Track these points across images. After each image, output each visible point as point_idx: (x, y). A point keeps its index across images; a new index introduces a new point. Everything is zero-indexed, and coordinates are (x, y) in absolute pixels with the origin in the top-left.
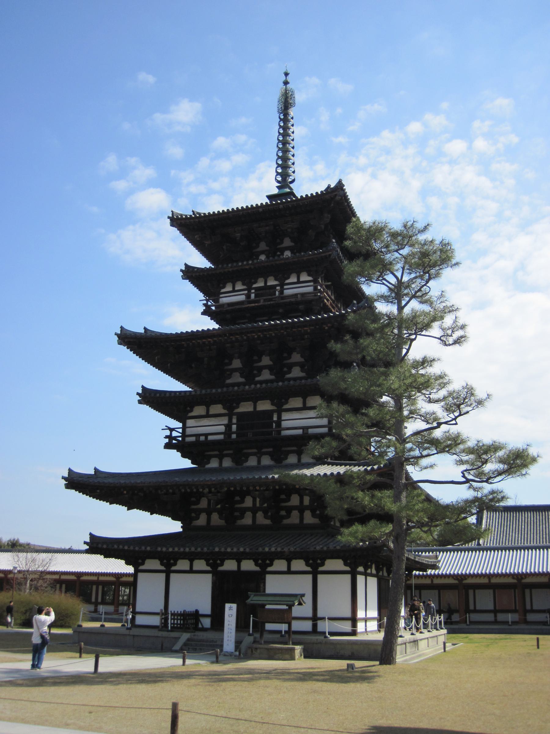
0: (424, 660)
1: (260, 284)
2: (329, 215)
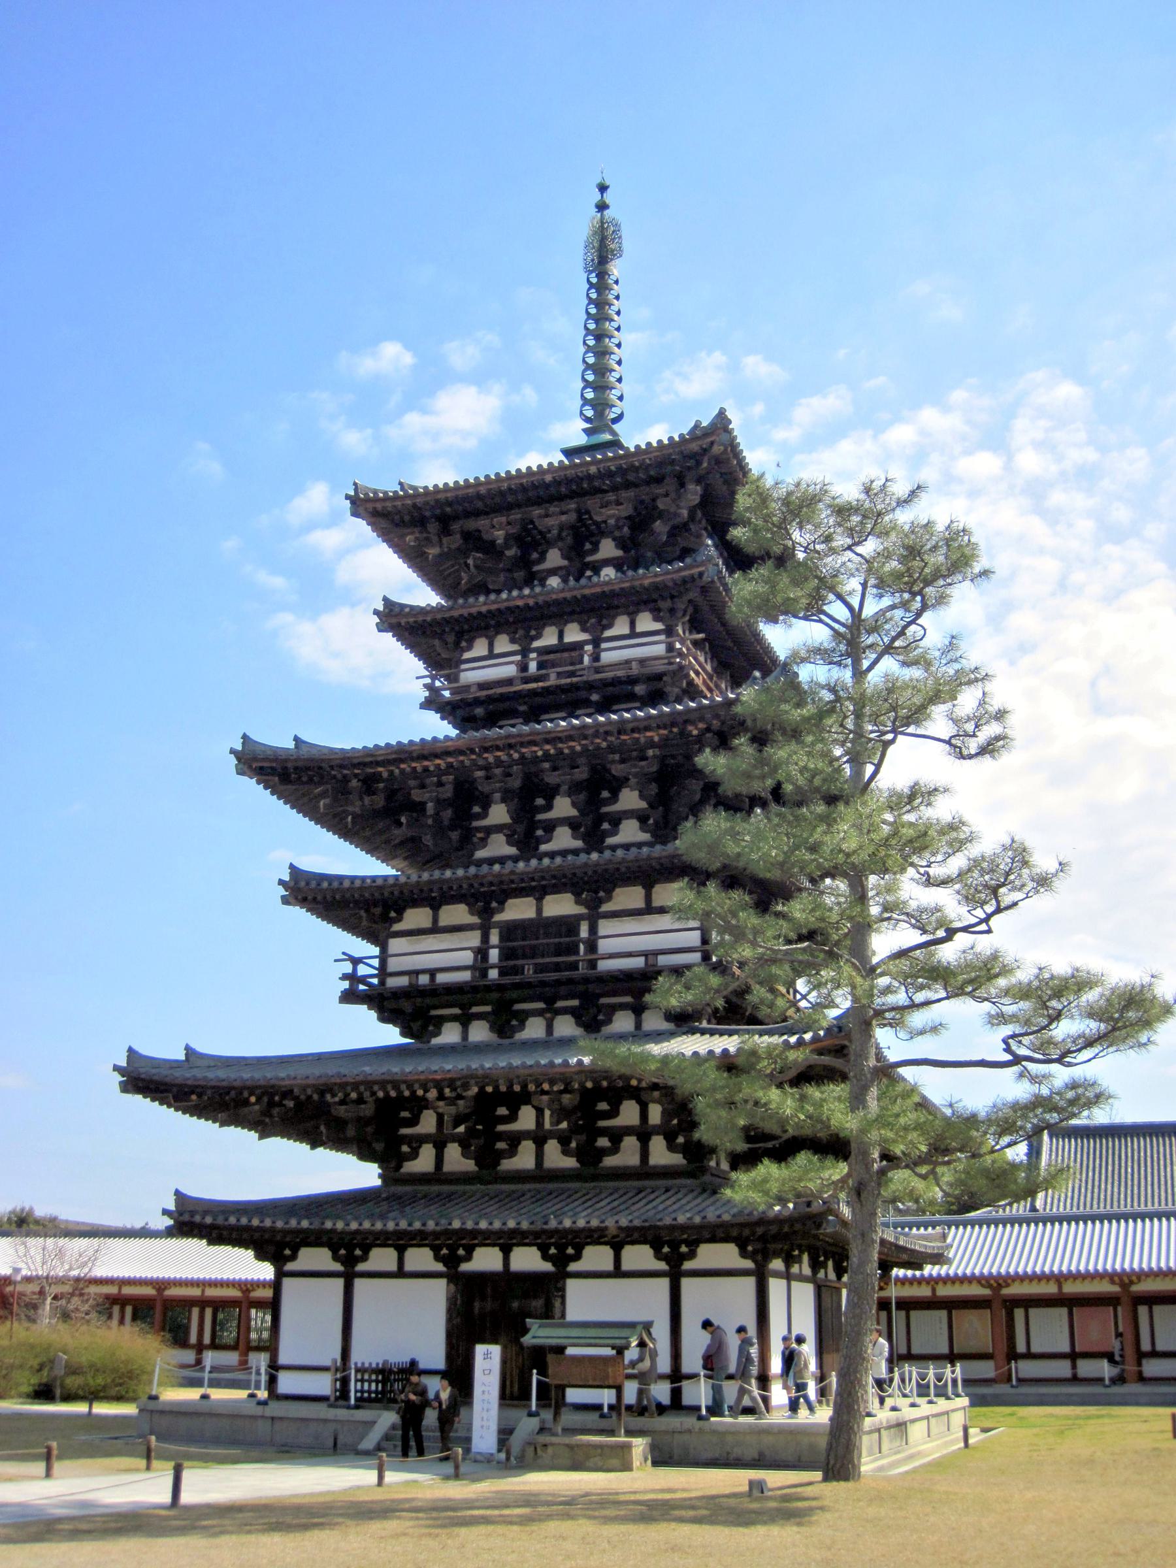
0: (921, 1466)
2: (698, 488)
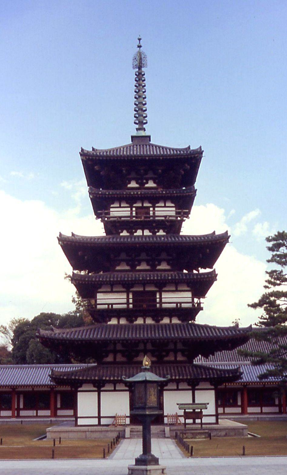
1: (139, 205)
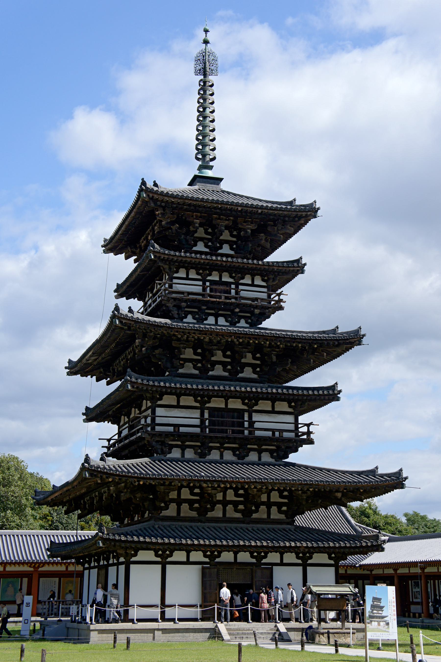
1: (215, 277)
